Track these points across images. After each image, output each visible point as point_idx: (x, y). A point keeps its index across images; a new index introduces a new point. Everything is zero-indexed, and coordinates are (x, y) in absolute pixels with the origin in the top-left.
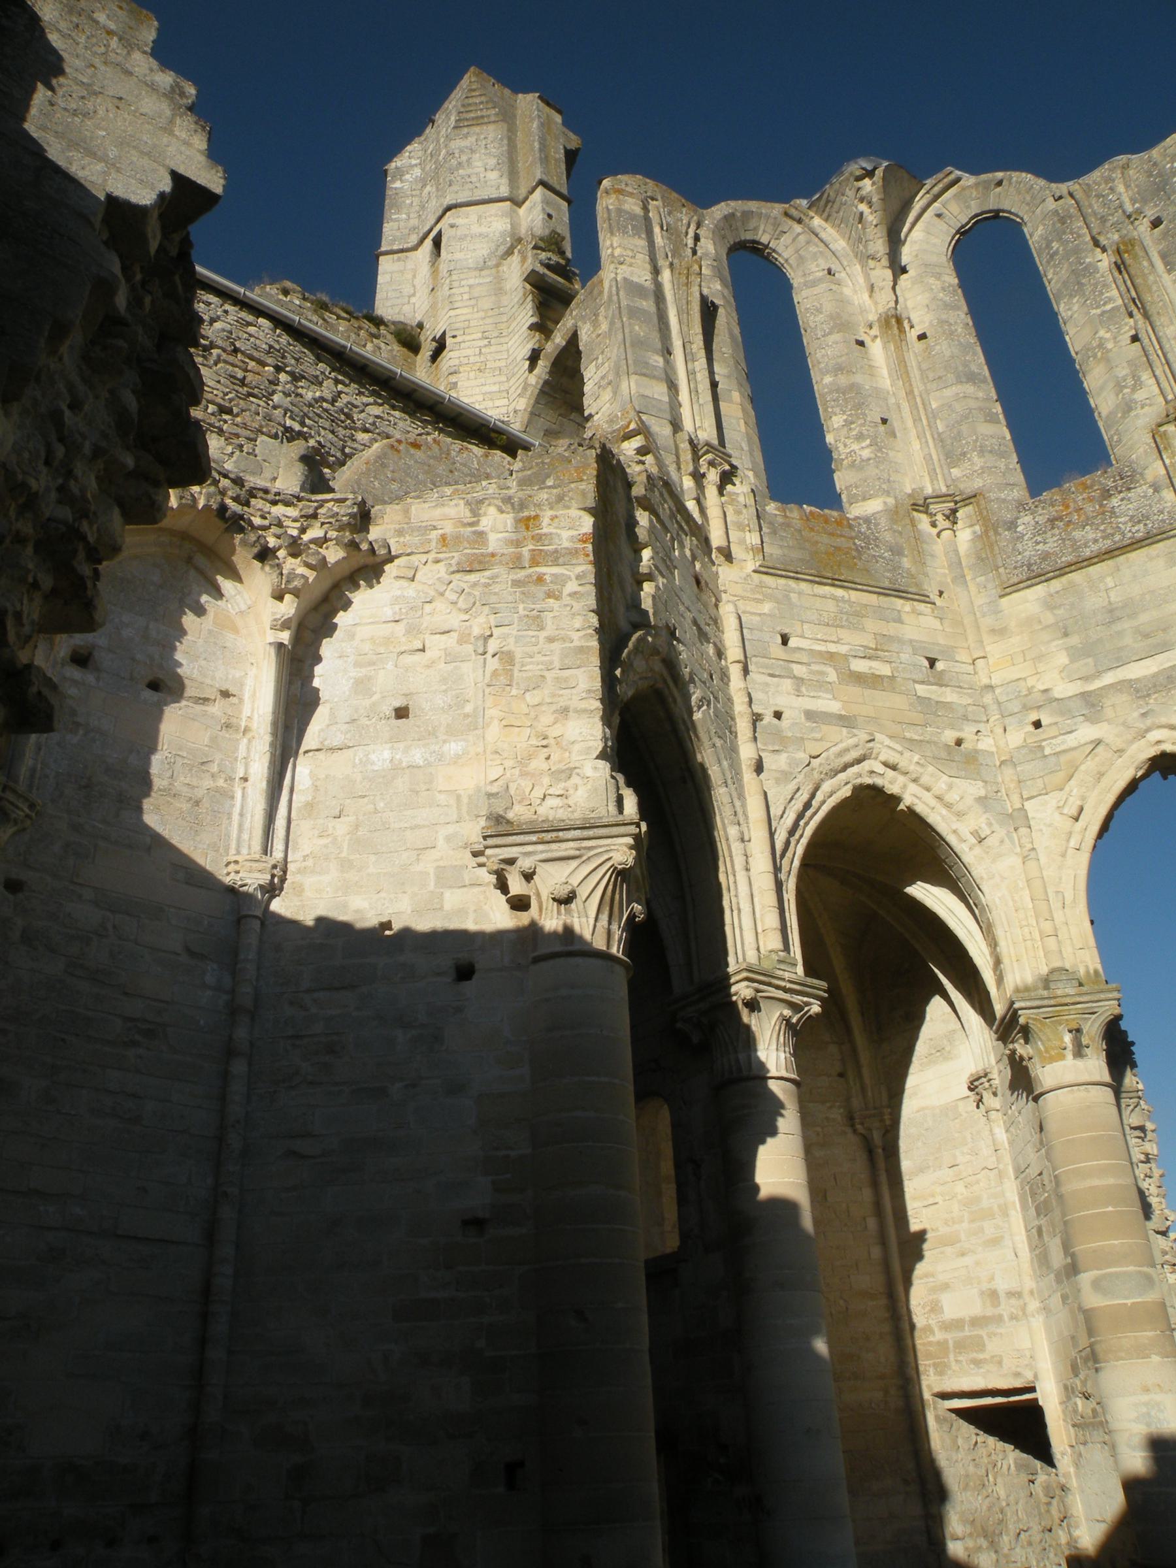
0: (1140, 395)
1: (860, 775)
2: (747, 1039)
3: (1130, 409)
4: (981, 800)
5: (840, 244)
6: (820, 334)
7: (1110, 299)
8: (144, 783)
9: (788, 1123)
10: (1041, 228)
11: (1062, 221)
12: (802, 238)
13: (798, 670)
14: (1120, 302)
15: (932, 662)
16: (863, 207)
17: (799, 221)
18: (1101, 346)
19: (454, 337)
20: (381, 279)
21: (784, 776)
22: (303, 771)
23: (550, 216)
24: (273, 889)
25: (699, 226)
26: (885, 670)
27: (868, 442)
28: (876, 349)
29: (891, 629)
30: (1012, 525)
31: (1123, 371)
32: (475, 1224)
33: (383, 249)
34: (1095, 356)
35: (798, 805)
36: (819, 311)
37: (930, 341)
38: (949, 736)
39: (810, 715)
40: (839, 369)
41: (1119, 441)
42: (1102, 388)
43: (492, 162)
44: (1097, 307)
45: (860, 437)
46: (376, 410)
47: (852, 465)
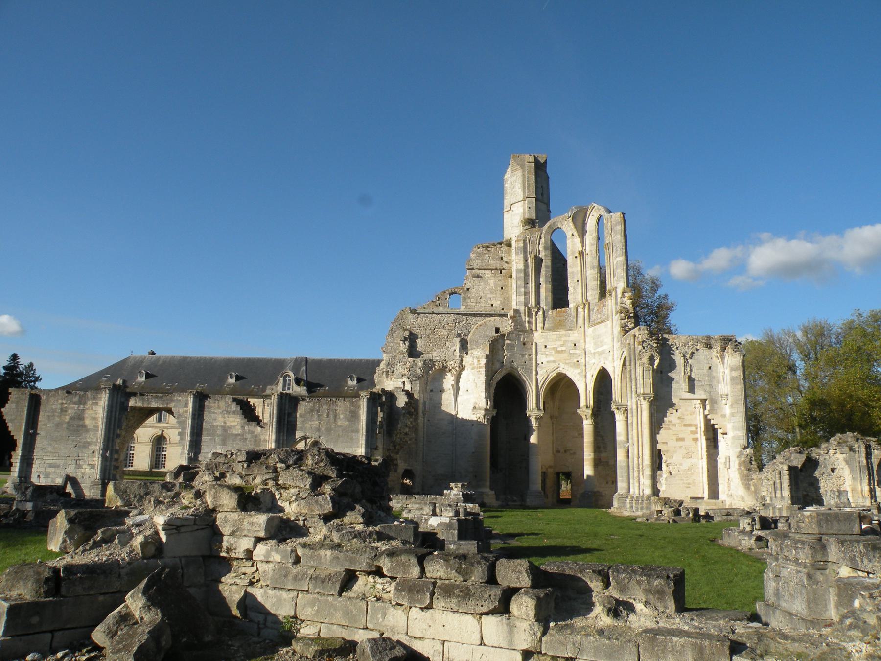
1: (556, 371)
2: (530, 421)
4: (579, 373)
8: (441, 405)
9: (535, 433)
13: (547, 353)
15: (575, 345)
20: (505, 221)
21: (542, 375)
22: (459, 398)
23: (529, 208)
24: (456, 415)
25: (541, 234)
26: (564, 348)
29: (567, 339)
30: (593, 309)
32: (473, 453)
33: (505, 210)
35: (544, 380)
38: (575, 360)
39: (548, 362)
43: (519, 185)
46: (474, 320)
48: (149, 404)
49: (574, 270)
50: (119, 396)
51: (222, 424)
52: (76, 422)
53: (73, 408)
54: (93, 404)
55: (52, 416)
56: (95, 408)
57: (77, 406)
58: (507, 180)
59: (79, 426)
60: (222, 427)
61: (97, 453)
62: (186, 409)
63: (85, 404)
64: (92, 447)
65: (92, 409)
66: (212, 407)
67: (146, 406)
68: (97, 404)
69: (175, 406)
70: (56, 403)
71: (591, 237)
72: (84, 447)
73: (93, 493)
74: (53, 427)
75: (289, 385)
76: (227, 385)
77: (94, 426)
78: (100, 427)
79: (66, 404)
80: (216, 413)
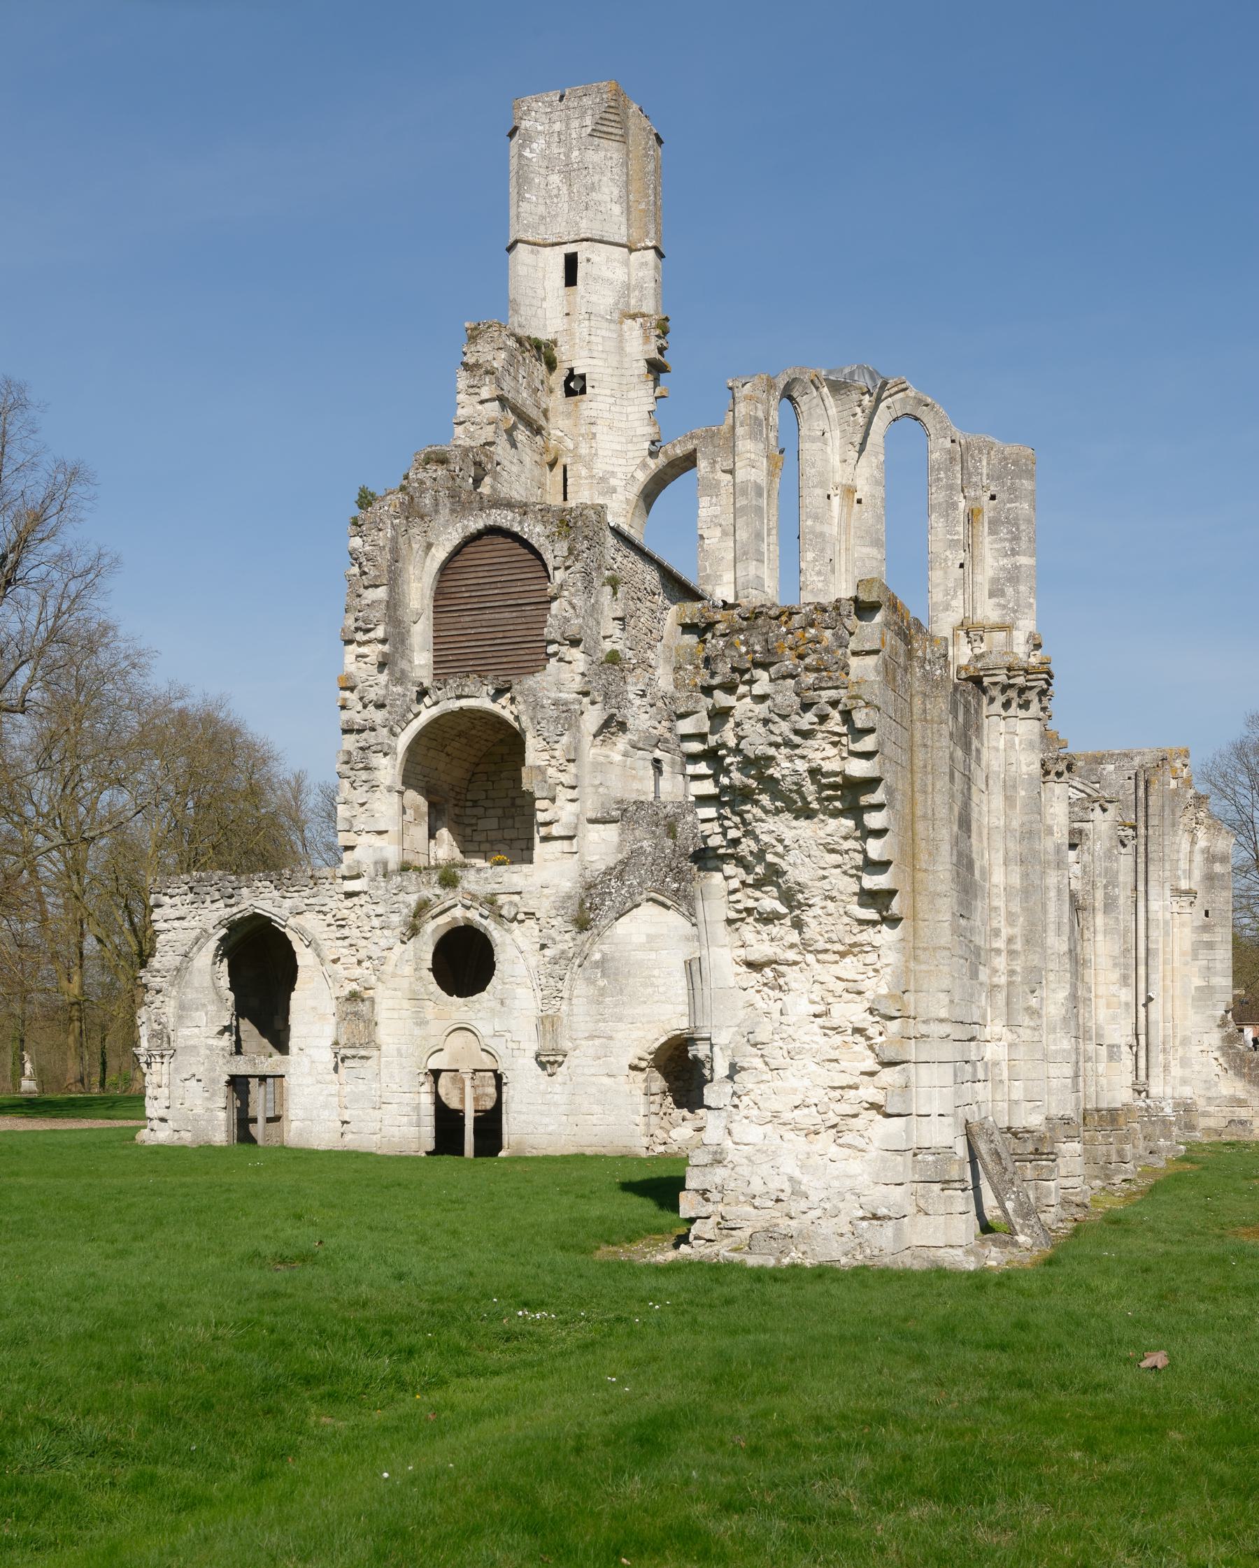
0: (954, 603)
3: (947, 610)
5: (833, 411)
6: (811, 484)
7: (958, 533)
10: (938, 454)
11: (952, 460)
12: (815, 401)
14: (962, 537)
16: (858, 410)
17: (817, 388)
18: (945, 560)
19: (593, 387)
27: (822, 578)
28: (836, 501)
31: (951, 585)
34: (940, 564)
36: (813, 465)
37: (863, 506)
40: (816, 518)
41: (937, 622)
42: (938, 585)
43: (616, 192)
44: (951, 534)
45: (819, 573)
47: (812, 591)
49: (825, 529)
58: (528, 139)
71: (874, 460)
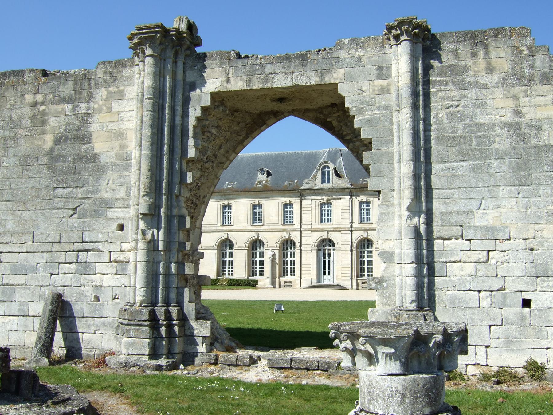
48: (266, 80)
50: (180, 65)
51: (509, 117)
52: (70, 149)
53: (58, 114)
54: (111, 97)
55: (12, 138)
56: (116, 106)
57: (70, 106)
59: (79, 159)
60: (508, 126)
61: (130, 228)
62: (384, 83)
63: (90, 98)
64: (116, 213)
65: (110, 109)
66: (466, 69)
67: (257, 85)
68: (121, 95)
69: (349, 78)
70: (19, 105)
72: (96, 213)
73: (128, 345)
74: (15, 166)
75: (329, 177)
76: (259, 182)
77: (118, 157)
78: (135, 154)
79: (43, 103)
80: (484, 86)
